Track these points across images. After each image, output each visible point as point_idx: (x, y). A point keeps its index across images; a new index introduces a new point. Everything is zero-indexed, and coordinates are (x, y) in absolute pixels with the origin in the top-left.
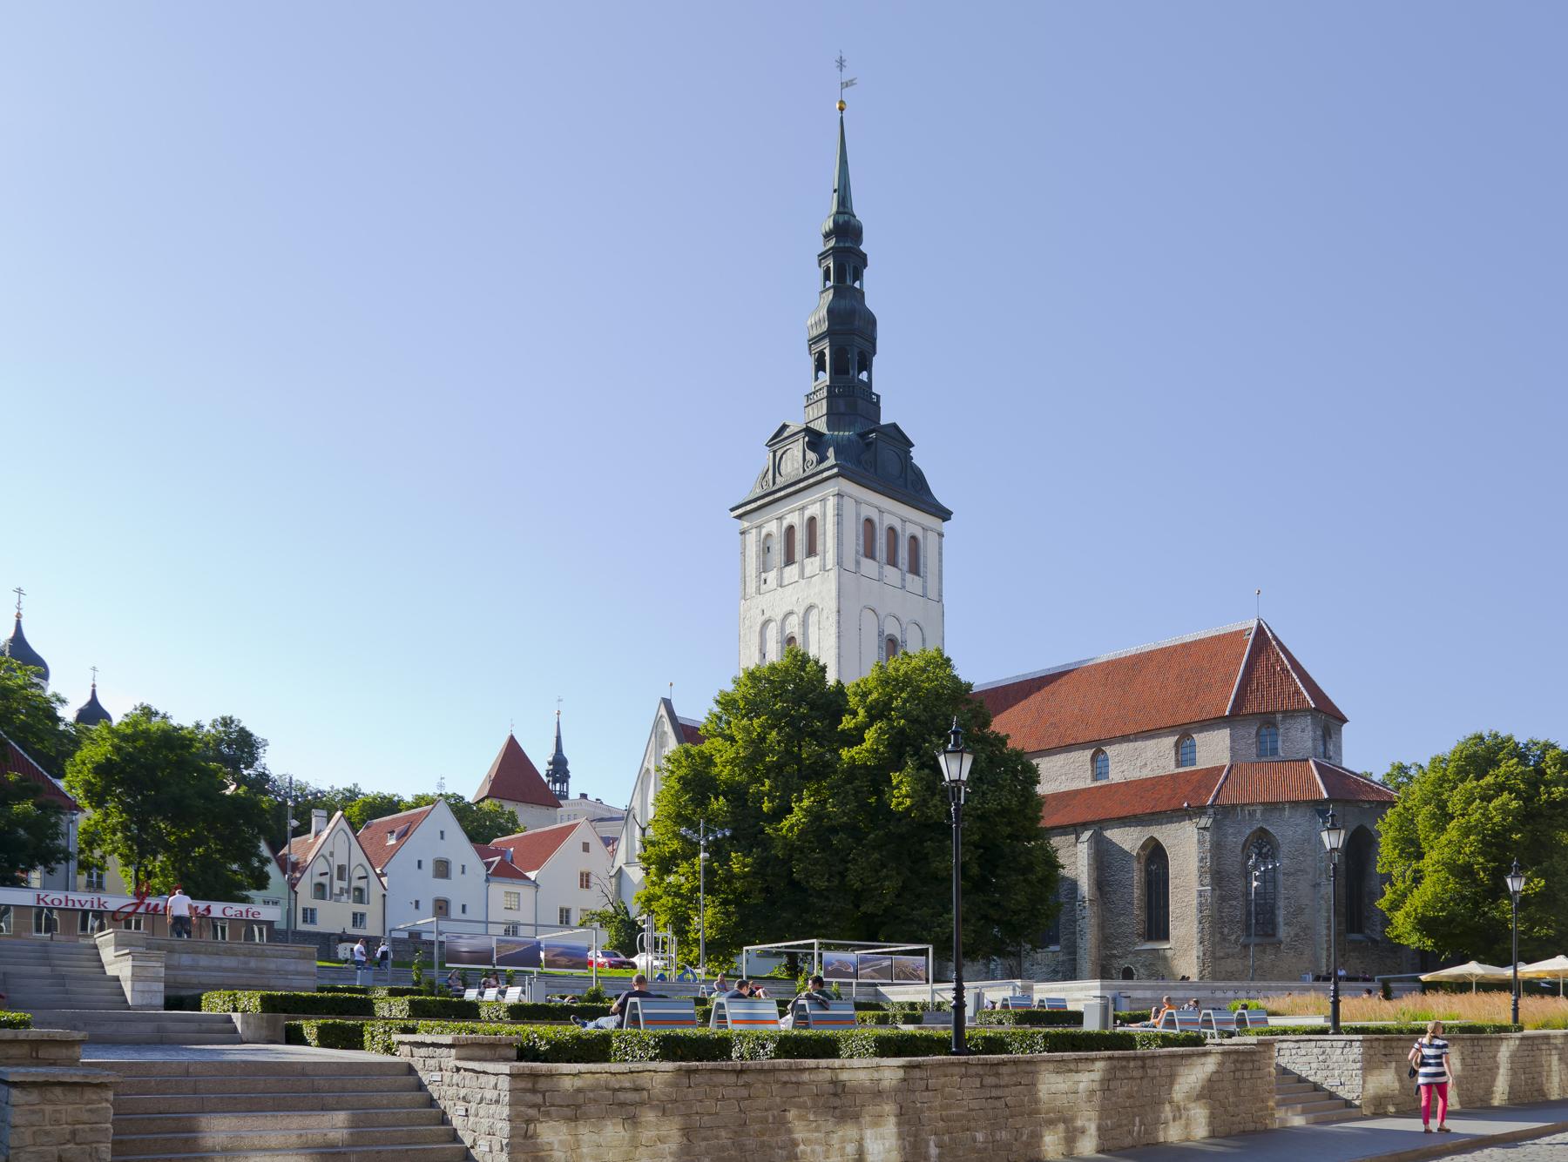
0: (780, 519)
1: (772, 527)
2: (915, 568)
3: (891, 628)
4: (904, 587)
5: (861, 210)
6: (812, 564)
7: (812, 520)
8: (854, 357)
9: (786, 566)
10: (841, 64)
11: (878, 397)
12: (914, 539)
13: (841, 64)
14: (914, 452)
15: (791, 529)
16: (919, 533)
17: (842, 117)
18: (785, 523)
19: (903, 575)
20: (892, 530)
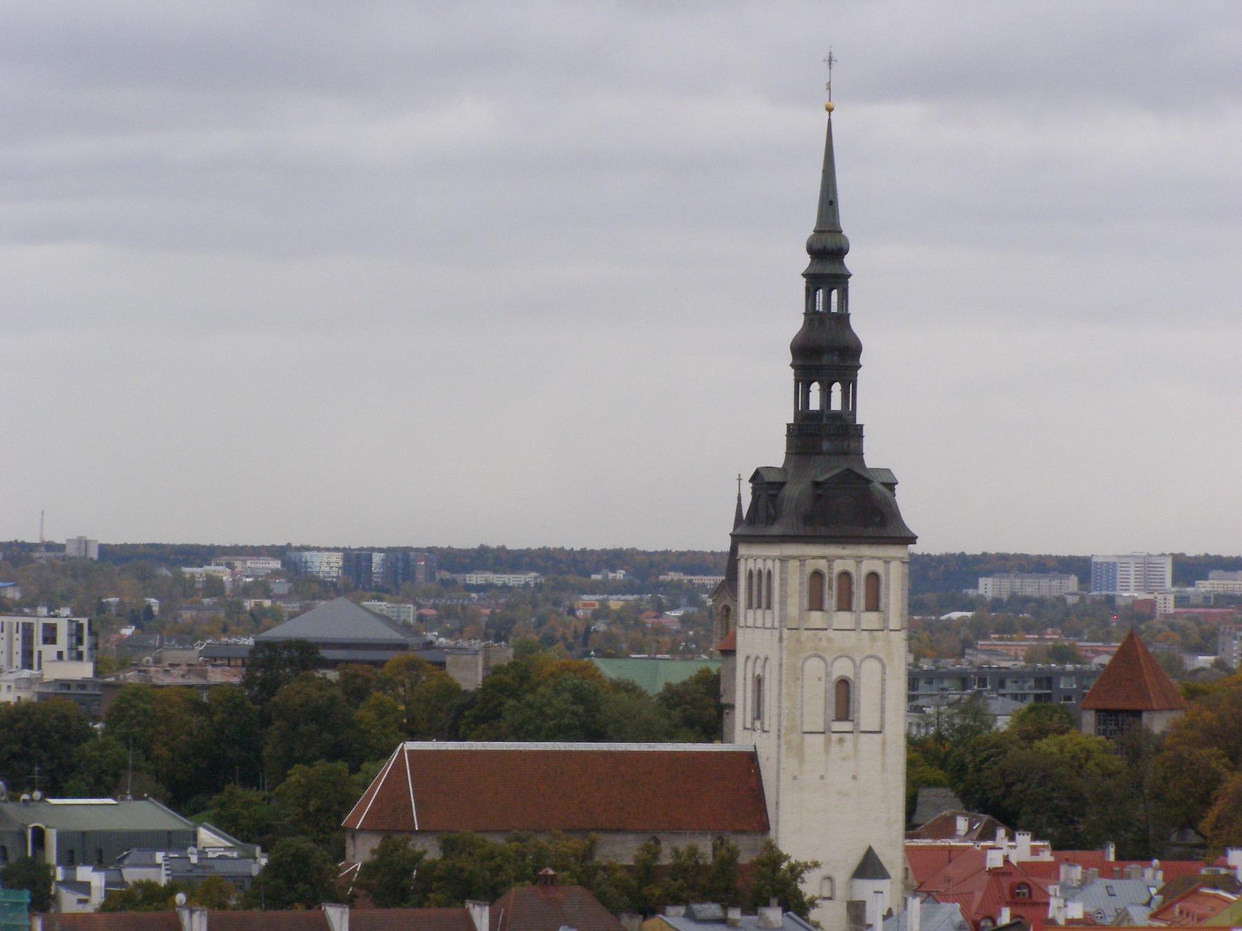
0: (830, 560)
1: (822, 565)
6: (871, 620)
17: (830, 120)
18: (839, 567)
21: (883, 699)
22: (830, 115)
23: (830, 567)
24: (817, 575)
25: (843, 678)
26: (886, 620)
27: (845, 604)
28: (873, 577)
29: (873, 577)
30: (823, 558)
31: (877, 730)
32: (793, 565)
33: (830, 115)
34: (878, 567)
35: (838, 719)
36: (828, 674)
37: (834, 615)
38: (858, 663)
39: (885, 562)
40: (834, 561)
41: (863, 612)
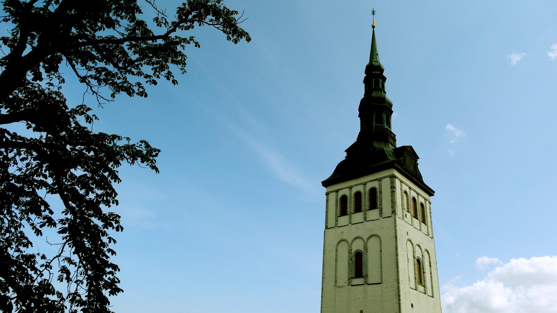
0: (351, 188)
1: (346, 192)
2: (424, 221)
3: (418, 254)
5: (383, 60)
6: (373, 214)
8: (384, 116)
9: (354, 213)
10: (373, 13)
11: (395, 135)
12: (422, 204)
13: (373, 13)
14: (419, 161)
16: (423, 202)
17: (373, 30)
18: (355, 190)
19: (420, 223)
21: (381, 261)
22: (373, 28)
26: (381, 213)
27: (358, 209)
28: (373, 191)
29: (373, 191)
30: (347, 188)
31: (380, 282)
33: (373, 28)
37: (353, 215)
38: (365, 241)
39: (378, 180)
40: (352, 188)
41: (367, 210)
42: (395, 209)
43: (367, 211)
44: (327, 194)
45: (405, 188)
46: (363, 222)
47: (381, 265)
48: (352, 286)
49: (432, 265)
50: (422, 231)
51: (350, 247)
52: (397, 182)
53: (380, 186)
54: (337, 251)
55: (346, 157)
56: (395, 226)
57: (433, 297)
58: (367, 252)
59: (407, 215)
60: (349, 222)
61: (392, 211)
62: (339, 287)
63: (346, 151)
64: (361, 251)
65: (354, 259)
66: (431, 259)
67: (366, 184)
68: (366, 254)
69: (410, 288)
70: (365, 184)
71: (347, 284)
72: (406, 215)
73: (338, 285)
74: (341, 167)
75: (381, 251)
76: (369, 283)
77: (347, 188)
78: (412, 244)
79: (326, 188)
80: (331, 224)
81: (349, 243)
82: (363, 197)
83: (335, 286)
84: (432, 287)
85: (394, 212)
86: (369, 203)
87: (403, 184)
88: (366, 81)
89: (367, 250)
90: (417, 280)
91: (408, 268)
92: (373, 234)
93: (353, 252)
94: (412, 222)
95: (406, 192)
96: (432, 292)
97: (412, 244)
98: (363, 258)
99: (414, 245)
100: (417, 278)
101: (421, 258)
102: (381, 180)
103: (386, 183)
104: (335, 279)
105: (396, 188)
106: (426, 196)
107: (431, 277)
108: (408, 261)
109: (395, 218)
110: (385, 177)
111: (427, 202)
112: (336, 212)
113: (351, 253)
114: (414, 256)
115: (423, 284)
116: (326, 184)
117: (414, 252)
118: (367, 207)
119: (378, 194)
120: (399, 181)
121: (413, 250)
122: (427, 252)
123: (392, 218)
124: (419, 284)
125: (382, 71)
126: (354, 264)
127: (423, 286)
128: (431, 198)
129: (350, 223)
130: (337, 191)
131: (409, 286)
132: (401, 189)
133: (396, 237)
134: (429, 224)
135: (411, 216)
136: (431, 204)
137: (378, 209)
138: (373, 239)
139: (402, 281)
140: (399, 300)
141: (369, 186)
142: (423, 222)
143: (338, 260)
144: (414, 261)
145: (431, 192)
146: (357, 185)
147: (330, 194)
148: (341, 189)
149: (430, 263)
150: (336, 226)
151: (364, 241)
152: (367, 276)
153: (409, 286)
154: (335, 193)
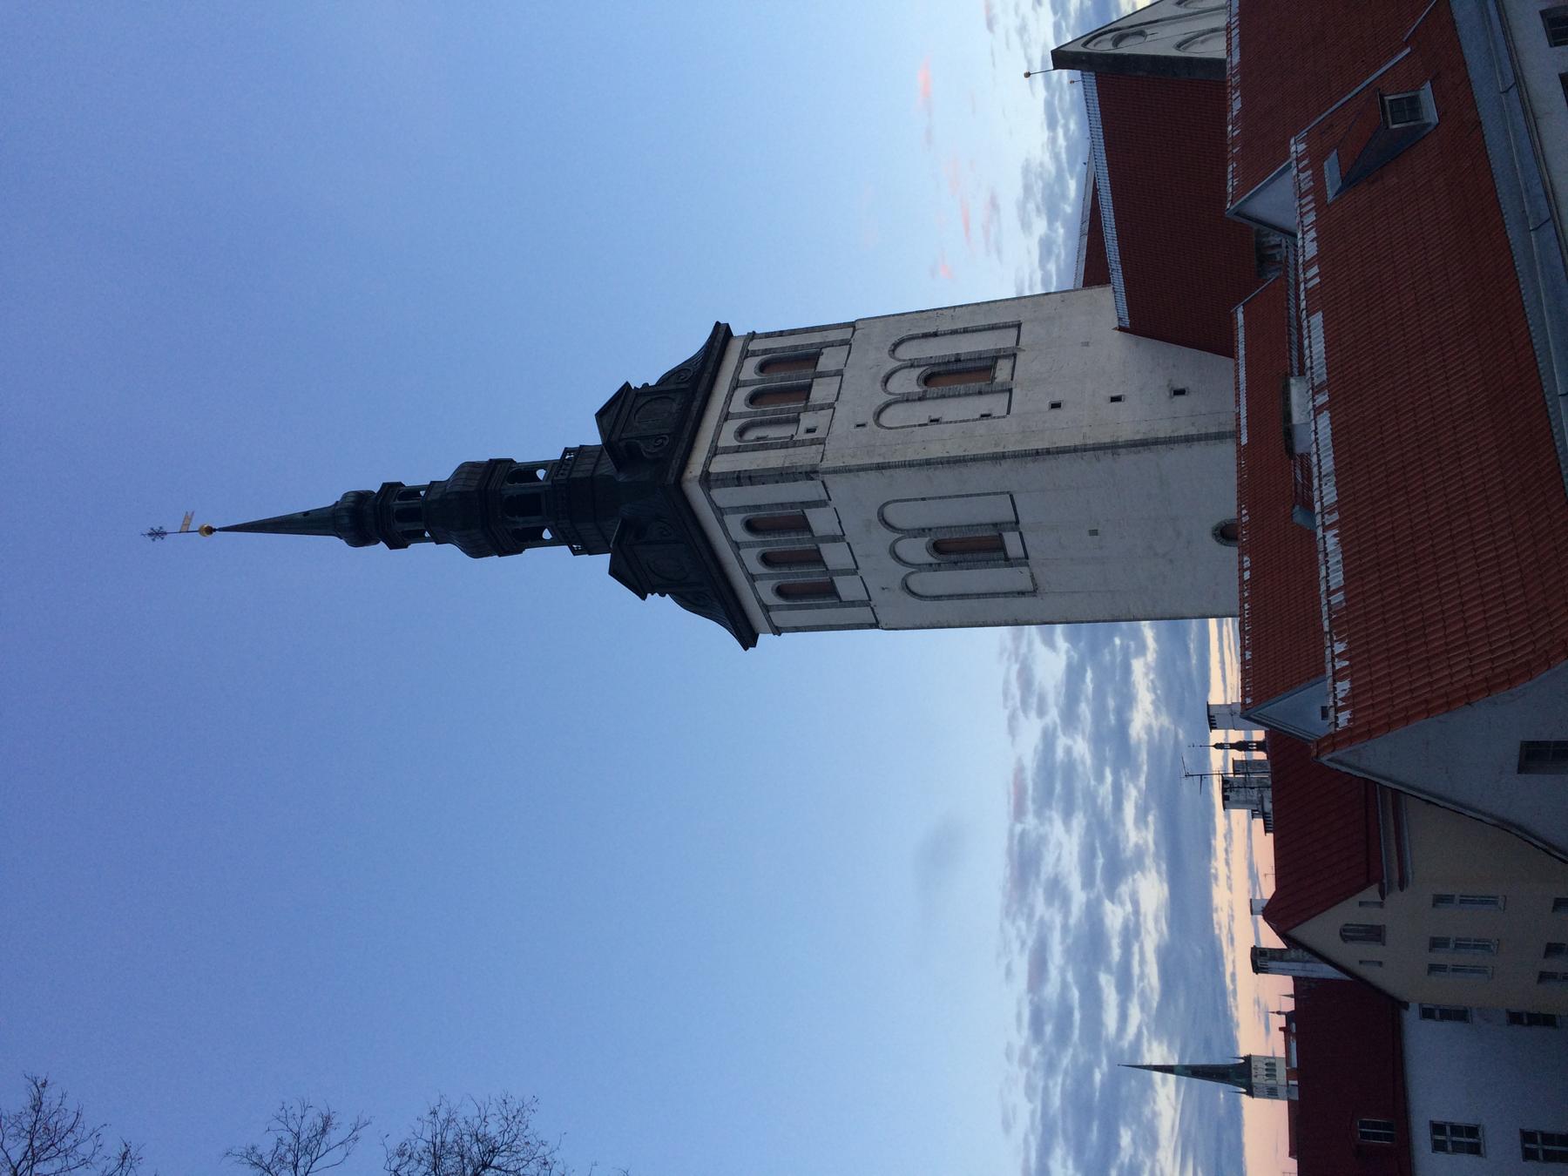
0: (752, 578)
1: (766, 590)
4: (840, 373)
5: (326, 497)
6: (821, 521)
7: (750, 526)
9: (824, 562)
10: (158, 534)
12: (762, 368)
13: (158, 534)
14: (636, 383)
15: (766, 559)
16: (752, 364)
18: (757, 568)
19: (822, 375)
20: (753, 399)
22: (215, 530)
23: (762, 577)
24: (780, 591)
25: (931, 545)
30: (754, 589)
31: (1008, 496)
32: (779, 618)
33: (215, 530)
34: (735, 523)
35: (1002, 548)
36: (930, 566)
37: (829, 568)
38: (901, 535)
39: (723, 515)
40: (752, 575)
41: (813, 536)
42: (800, 473)
43: (816, 535)
44: (777, 631)
45: (728, 438)
46: (848, 544)
47: (963, 496)
48: (1027, 557)
49: (932, 330)
50: (841, 367)
51: (920, 567)
52: (721, 465)
53: (736, 510)
54: (938, 598)
55: (662, 595)
56: (847, 470)
57: (1018, 326)
58: (930, 529)
59: (810, 426)
60: (853, 574)
61: (807, 480)
62: (1035, 585)
63: (643, 597)
64: (929, 541)
65: (953, 557)
66: (914, 332)
67: (736, 543)
68: (936, 533)
69: (1008, 412)
70: (737, 546)
71: (1025, 569)
72: (809, 431)
73: (1030, 587)
74: (694, 601)
75: (923, 499)
76: (1014, 519)
77: (754, 589)
78: (887, 405)
79: (758, 635)
80: (864, 614)
81: (913, 573)
82: (776, 548)
83: (1034, 592)
84: (993, 328)
85: (810, 474)
86: (792, 534)
87: (721, 444)
88: (397, 542)
89: (923, 530)
90: (982, 385)
91: (956, 422)
92: (880, 520)
93: (931, 560)
94: (823, 409)
95: (741, 432)
96: (1006, 326)
97: (887, 405)
98: (947, 537)
99: (886, 398)
100: (974, 386)
101: (918, 371)
102: (719, 508)
103: (723, 496)
104: (1014, 597)
105: (739, 471)
106: (734, 351)
107: (966, 331)
108: (937, 421)
109: (826, 472)
110: (711, 502)
111: (753, 346)
112: (828, 606)
113: (939, 564)
114: (920, 399)
115: (989, 363)
116: (748, 638)
117: (907, 401)
118: (807, 536)
119: (762, 513)
120: (713, 461)
121: (902, 402)
122: (896, 345)
123: (827, 478)
124: (994, 378)
125: (362, 497)
126: (968, 556)
127: (996, 363)
128: (738, 330)
129: (854, 572)
130: (766, 609)
131: (1004, 417)
132: (737, 452)
133: (880, 467)
134: (816, 338)
135: (806, 409)
136: (754, 332)
137: (806, 511)
138: (891, 513)
139: (996, 445)
140: (1048, 452)
141: (742, 535)
142: (815, 368)
143: (960, 591)
144: (934, 398)
145: (721, 336)
146: (743, 565)
147: (776, 625)
148: (760, 600)
149: (926, 336)
150: (869, 605)
151: (899, 539)
152: (995, 525)
153: (1004, 417)
154: (770, 613)
